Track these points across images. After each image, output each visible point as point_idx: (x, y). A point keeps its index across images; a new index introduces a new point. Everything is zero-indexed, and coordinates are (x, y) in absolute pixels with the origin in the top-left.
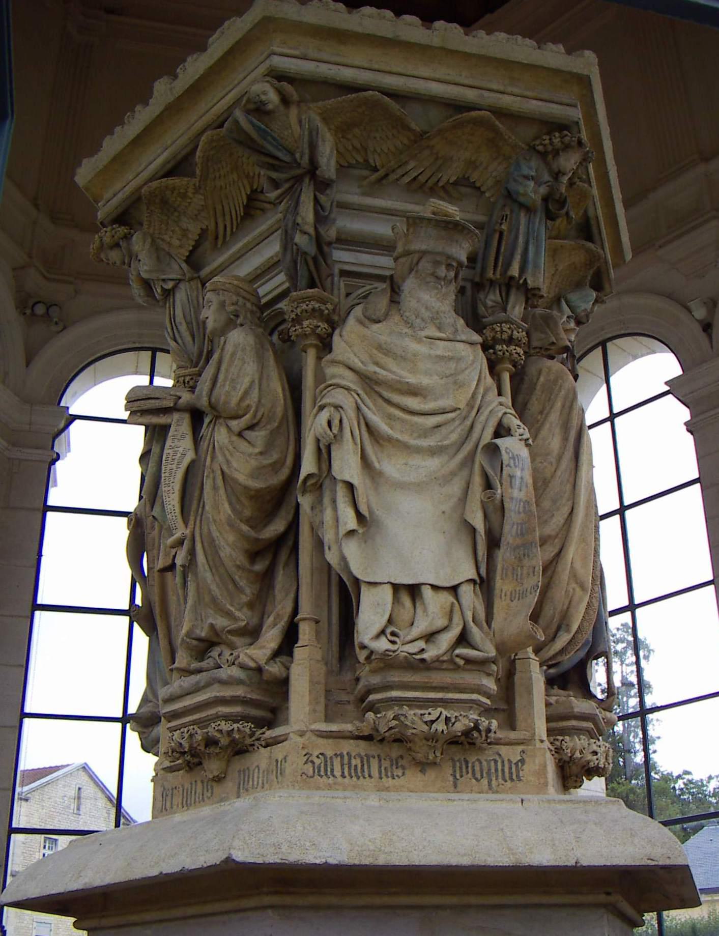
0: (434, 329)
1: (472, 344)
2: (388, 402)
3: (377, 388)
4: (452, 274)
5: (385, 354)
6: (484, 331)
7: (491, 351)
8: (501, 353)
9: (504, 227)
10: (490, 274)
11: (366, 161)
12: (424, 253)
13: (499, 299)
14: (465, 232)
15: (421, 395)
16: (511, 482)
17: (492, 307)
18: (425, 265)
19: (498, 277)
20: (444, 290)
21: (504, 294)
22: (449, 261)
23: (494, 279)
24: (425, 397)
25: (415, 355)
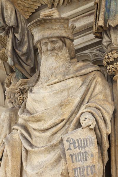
4: (60, 43)
5: (36, 102)
8: (110, 70)
11: (42, 4)
14: (48, 21)
16: (72, 159)
17: (108, 45)
24: (45, 121)
25: (43, 98)
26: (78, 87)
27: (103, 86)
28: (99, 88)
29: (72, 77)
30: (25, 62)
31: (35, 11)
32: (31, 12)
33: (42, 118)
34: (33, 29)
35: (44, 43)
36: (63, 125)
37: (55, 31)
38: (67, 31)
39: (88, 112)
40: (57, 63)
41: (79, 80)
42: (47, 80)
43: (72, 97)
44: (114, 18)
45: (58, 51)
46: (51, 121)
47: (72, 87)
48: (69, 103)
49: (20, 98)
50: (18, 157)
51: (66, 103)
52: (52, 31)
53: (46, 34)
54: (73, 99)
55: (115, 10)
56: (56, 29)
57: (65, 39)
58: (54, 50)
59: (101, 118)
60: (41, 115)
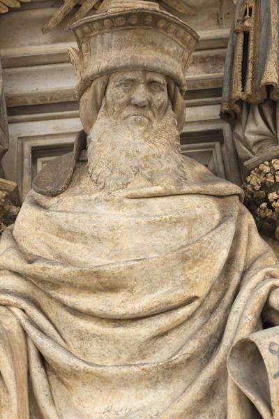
0: (144, 182)
1: (218, 196)
2: (75, 312)
3: (54, 293)
4: (161, 97)
5: (70, 239)
6: (248, 179)
7: (264, 205)
9: (247, 24)
10: (238, 93)
12: (108, 73)
13: (266, 129)
14: (161, 24)
15: (125, 287)
17: (257, 143)
18: (115, 92)
19: (249, 90)
20: (155, 125)
21: (269, 120)
22: (149, 76)
23: (244, 97)
24: (131, 290)
25: (112, 229)
29: (198, 194)
31: (18, 5)
32: (7, 4)
33: (125, 283)
34: (103, 34)
35: (127, 80)
36: (190, 314)
37: (167, 57)
40: (151, 145)
42: (125, 183)
43: (209, 243)
48: (203, 257)
50: (23, 389)
52: (160, 54)
53: (144, 57)
54: (212, 248)
56: (168, 53)
58: (146, 108)
60: (126, 273)
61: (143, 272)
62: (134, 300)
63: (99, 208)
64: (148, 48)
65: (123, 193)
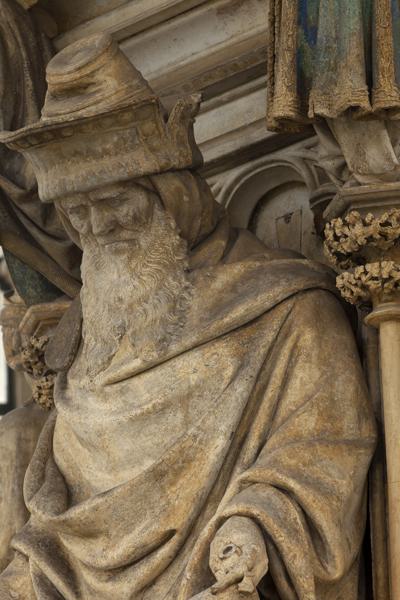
15: (101, 532)
24: (108, 535)
26: (223, 387)
27: (323, 362)
28: (305, 377)
29: (196, 346)
30: (40, 224)
36: (172, 553)
37: (107, 162)
38: (156, 143)
39: (239, 514)
41: (223, 354)
43: (195, 436)
44: (334, 76)
45: (133, 230)
46: (131, 536)
47: (197, 386)
48: (188, 461)
49: (40, 388)
51: (177, 462)
52: (94, 162)
53: (72, 177)
54: (200, 443)
55: (337, 38)
56: (106, 152)
57: (155, 179)
59: (293, 532)
61: (110, 511)
62: (114, 546)
63: (90, 399)
64: (73, 162)
65: (101, 379)
